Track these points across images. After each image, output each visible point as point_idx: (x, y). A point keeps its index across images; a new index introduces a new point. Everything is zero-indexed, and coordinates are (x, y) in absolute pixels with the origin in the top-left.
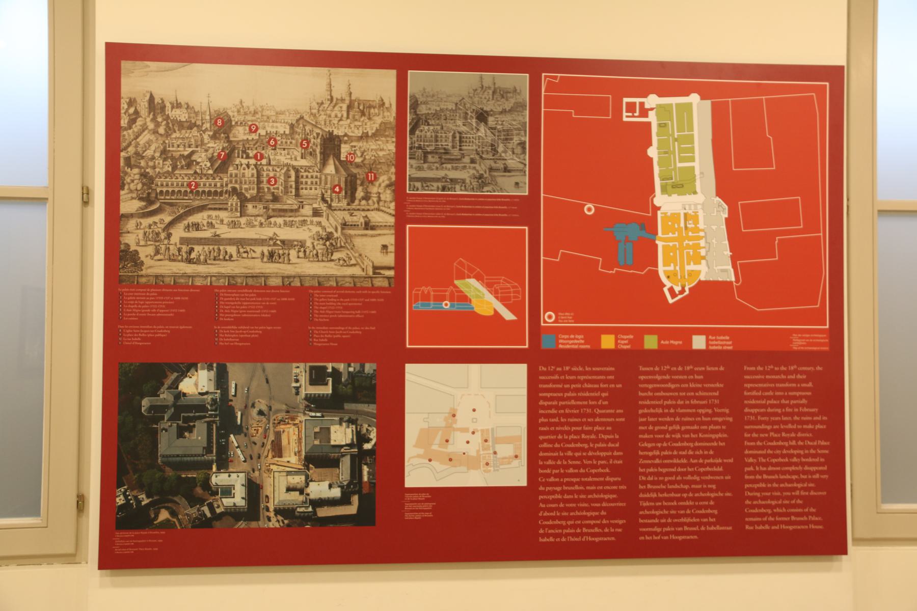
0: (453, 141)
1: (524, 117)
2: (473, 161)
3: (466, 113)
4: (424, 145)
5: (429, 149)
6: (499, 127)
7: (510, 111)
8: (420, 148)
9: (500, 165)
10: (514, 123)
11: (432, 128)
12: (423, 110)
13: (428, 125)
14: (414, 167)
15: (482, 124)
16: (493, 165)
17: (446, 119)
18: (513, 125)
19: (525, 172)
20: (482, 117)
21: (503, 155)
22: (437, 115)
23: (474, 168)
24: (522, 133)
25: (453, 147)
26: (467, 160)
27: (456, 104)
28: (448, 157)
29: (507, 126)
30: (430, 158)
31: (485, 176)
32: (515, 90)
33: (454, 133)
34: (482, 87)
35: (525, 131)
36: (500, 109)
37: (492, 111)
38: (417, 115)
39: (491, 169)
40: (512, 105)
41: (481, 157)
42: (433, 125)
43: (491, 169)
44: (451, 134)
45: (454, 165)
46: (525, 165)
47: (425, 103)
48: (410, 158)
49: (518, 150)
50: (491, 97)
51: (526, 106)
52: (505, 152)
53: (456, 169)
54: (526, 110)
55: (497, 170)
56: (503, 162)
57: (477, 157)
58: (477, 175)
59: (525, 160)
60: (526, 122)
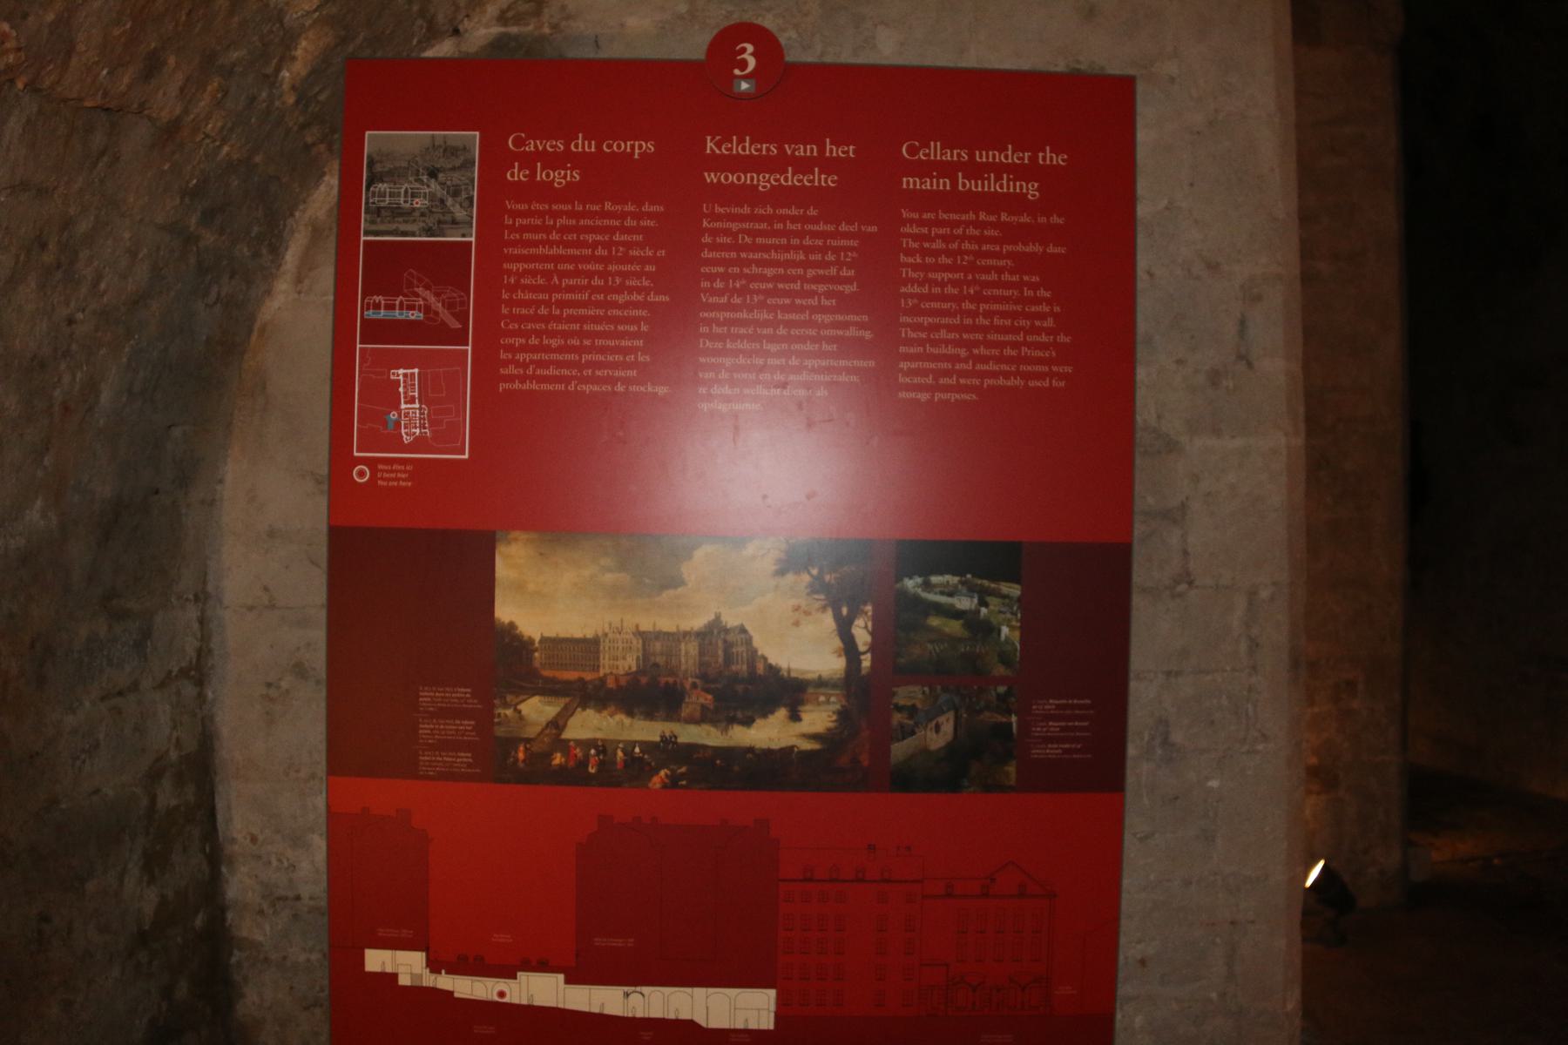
0: (406, 195)
1: (474, 172)
2: (423, 215)
3: (419, 171)
4: (378, 201)
5: (382, 204)
6: (449, 183)
7: (459, 167)
8: (374, 203)
9: (448, 218)
10: (463, 178)
11: (385, 185)
12: (378, 168)
13: (382, 182)
14: (368, 219)
15: (433, 180)
16: (442, 218)
17: (399, 176)
18: (460, 180)
19: (472, 224)
20: (433, 174)
21: (451, 208)
22: (391, 173)
23: (424, 221)
24: (470, 188)
25: (406, 202)
26: (417, 214)
27: (409, 162)
28: (401, 211)
29: (455, 181)
30: (383, 211)
31: (434, 228)
32: (465, 148)
33: (407, 189)
34: (434, 146)
35: (473, 186)
36: (450, 166)
37: (442, 167)
38: (372, 173)
39: (440, 222)
40: (461, 161)
41: (431, 212)
42: (386, 182)
43: (440, 222)
44: (403, 191)
45: (406, 219)
46: (472, 218)
47: (381, 162)
48: (366, 213)
49: (466, 204)
50: (442, 154)
51: (474, 162)
52: (453, 206)
53: (406, 222)
54: (474, 165)
55: (445, 222)
56: (450, 215)
57: (427, 211)
58: (426, 227)
59: (472, 212)
60: (474, 178)
